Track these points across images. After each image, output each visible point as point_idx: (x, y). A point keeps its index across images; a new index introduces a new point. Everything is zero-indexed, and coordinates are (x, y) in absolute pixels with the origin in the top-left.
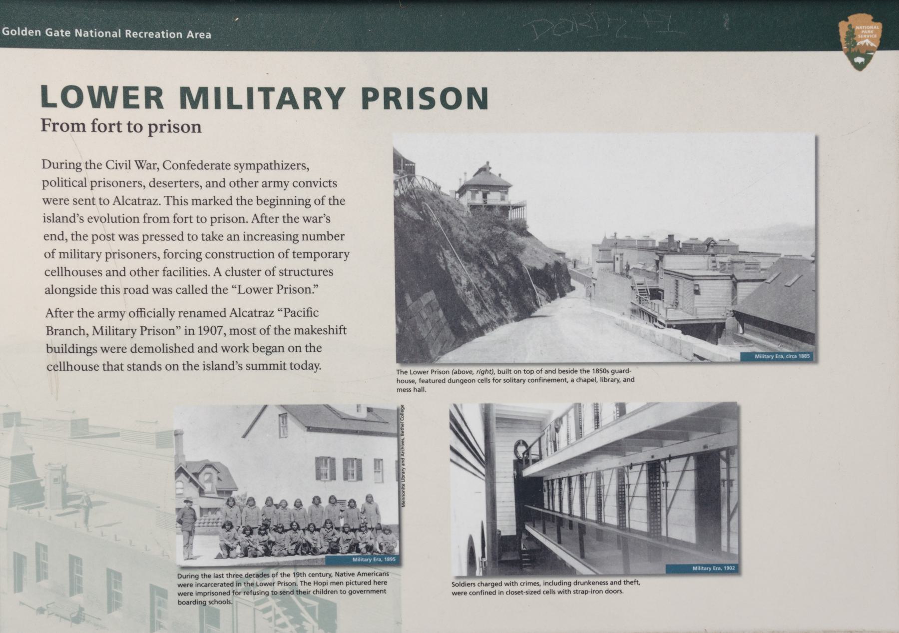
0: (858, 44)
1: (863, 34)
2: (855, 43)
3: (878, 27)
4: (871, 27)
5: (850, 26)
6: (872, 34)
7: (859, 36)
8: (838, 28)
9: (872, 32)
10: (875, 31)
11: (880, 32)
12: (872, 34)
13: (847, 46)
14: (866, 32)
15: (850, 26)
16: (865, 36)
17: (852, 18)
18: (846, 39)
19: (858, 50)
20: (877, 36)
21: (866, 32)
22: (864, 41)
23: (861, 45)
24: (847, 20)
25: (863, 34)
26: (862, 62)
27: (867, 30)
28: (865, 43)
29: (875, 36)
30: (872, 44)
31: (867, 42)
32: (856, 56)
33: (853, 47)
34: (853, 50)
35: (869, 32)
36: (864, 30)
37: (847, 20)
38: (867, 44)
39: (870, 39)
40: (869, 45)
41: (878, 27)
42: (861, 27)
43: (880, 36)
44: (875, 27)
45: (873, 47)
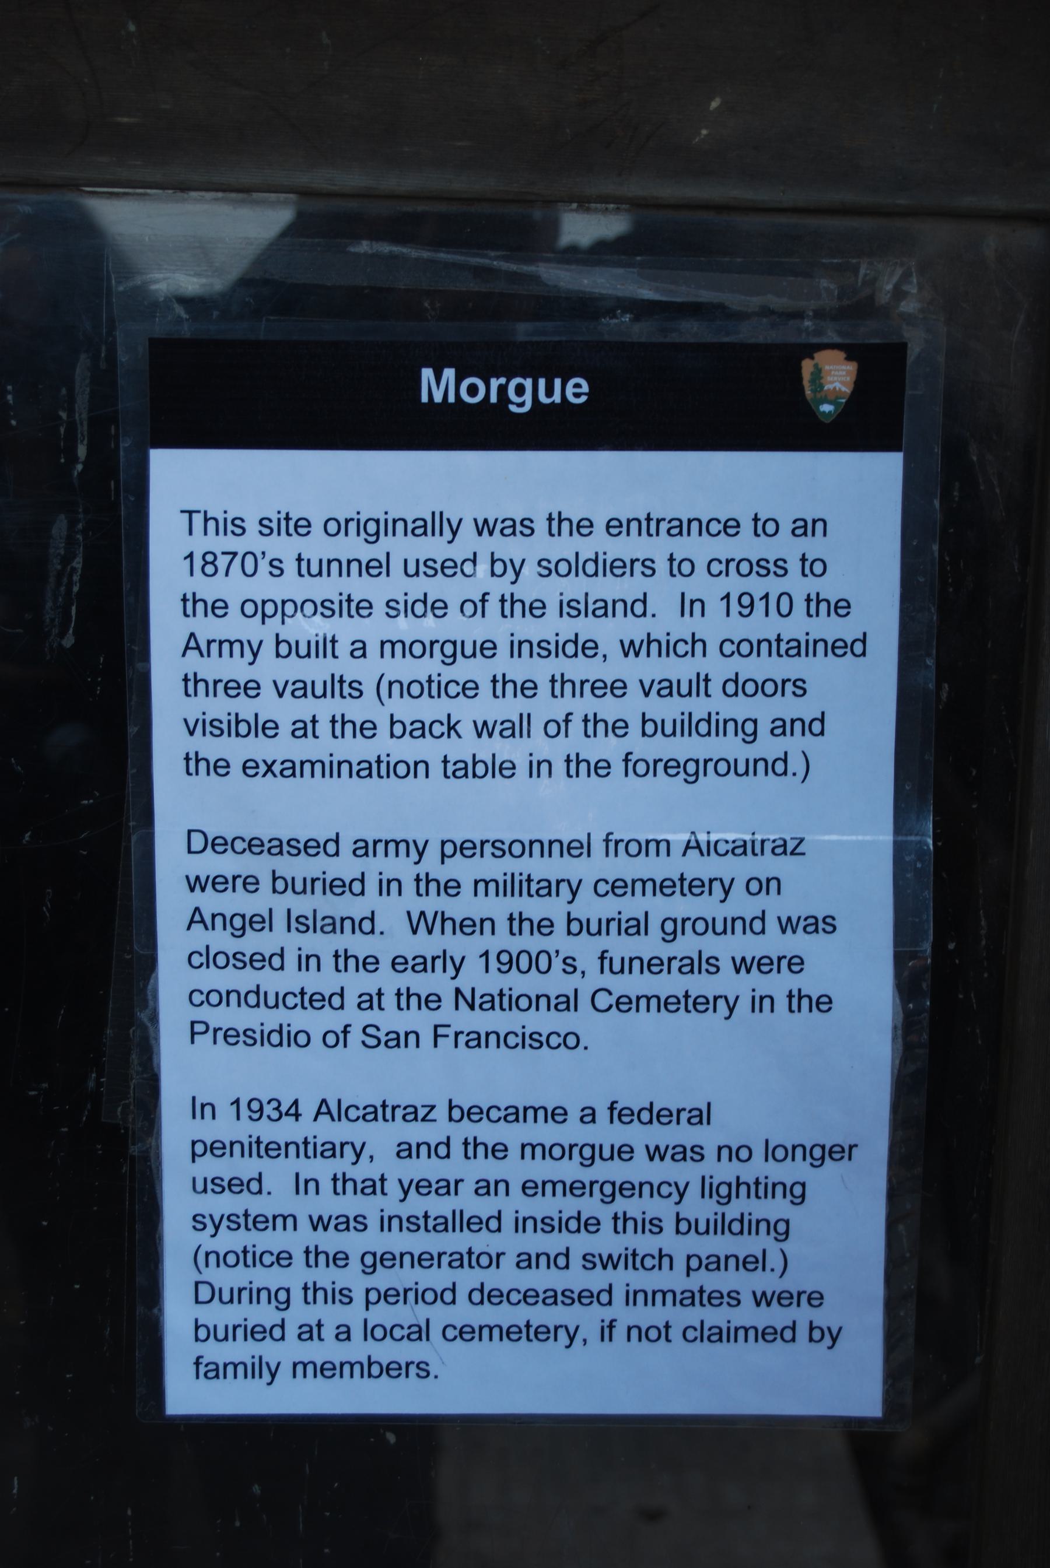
0: (826, 388)
1: (834, 376)
2: (822, 386)
3: (852, 367)
4: (844, 367)
5: (816, 366)
6: (844, 376)
7: (829, 379)
8: (800, 368)
9: (844, 373)
10: (848, 372)
11: (855, 372)
12: (844, 376)
13: (811, 390)
14: (837, 373)
15: (816, 366)
16: (835, 378)
17: (821, 357)
18: (809, 382)
19: (826, 396)
20: (850, 379)
21: (837, 373)
22: (834, 385)
23: (829, 390)
24: (812, 358)
25: (834, 376)
26: (830, 412)
27: (838, 371)
28: (835, 388)
29: (848, 379)
30: (844, 389)
31: (838, 385)
32: (823, 403)
33: (819, 392)
34: (819, 396)
35: (841, 373)
36: (835, 371)
37: (812, 358)
38: (837, 389)
39: (842, 383)
40: (840, 389)
41: (852, 367)
42: (831, 367)
43: (854, 379)
44: (848, 367)
45: (845, 392)
